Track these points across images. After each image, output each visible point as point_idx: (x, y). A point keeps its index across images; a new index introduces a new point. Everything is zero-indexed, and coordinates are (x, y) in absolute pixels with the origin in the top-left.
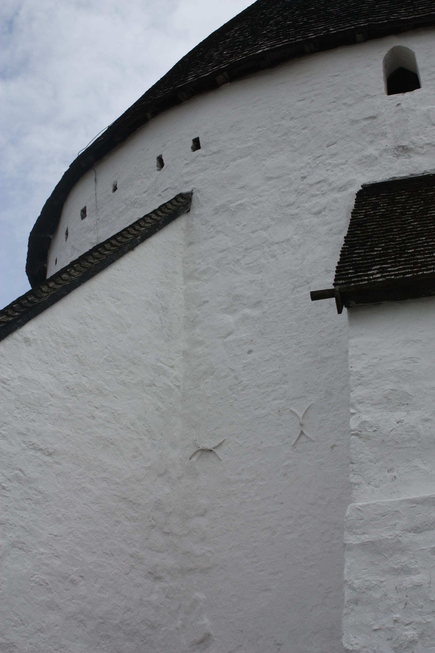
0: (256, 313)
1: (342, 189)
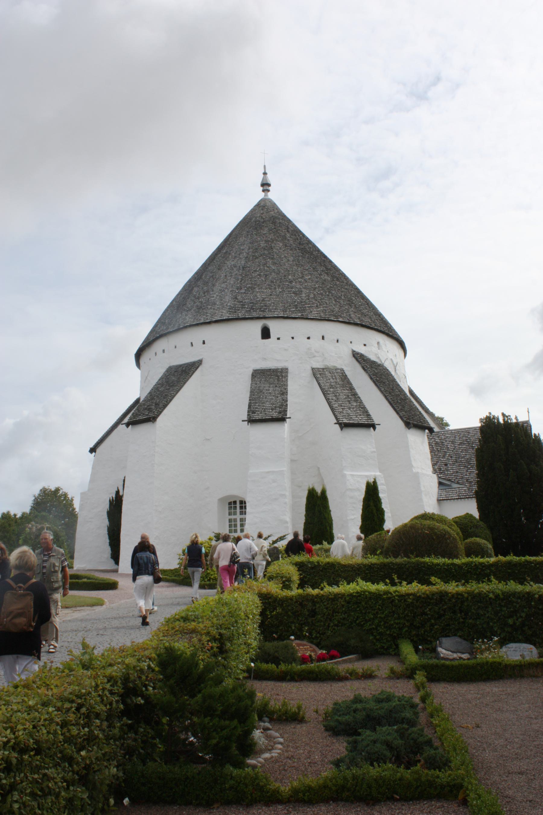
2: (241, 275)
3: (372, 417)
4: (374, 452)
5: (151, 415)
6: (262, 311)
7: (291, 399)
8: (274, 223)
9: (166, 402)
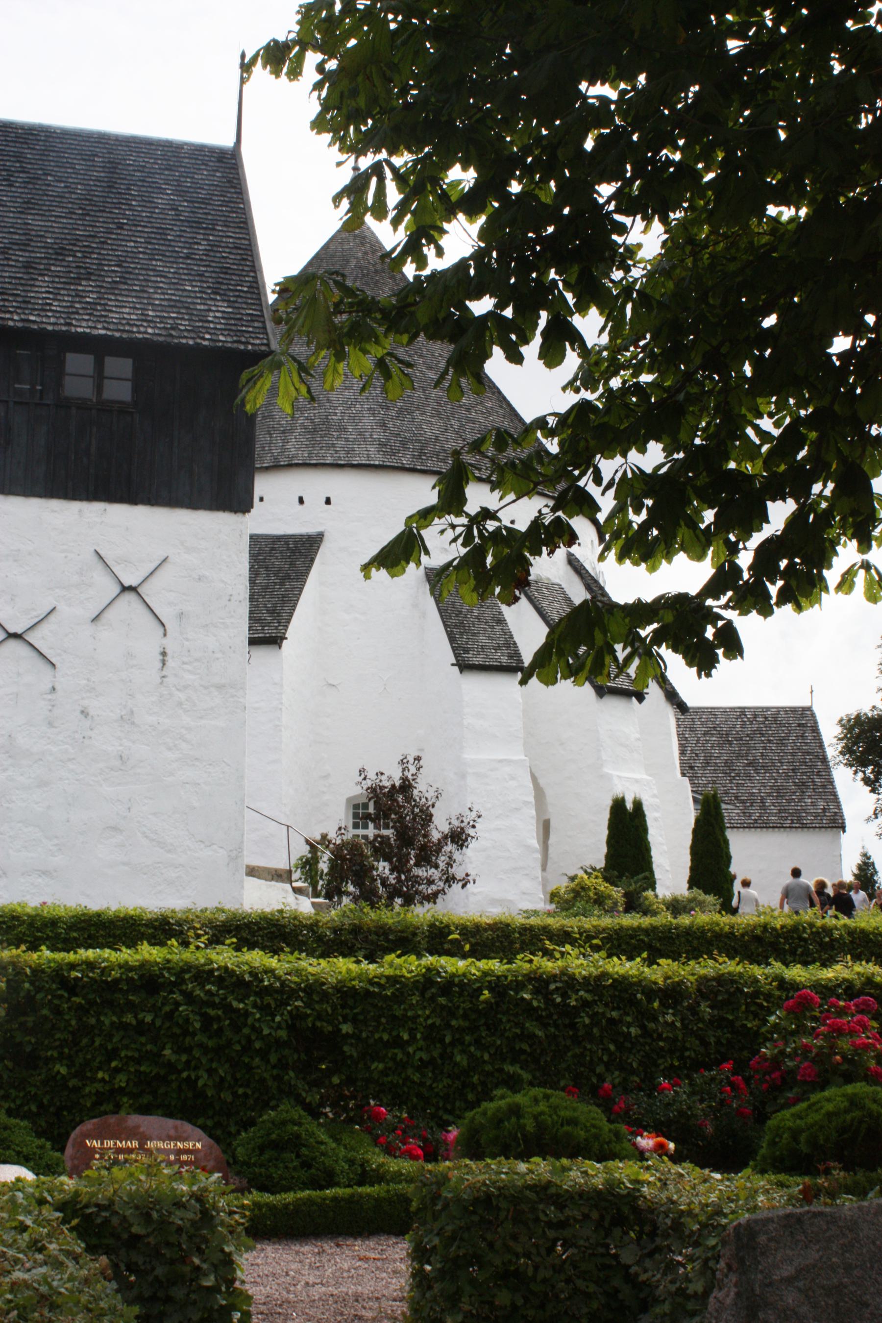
4: (638, 739)
5: (269, 632)
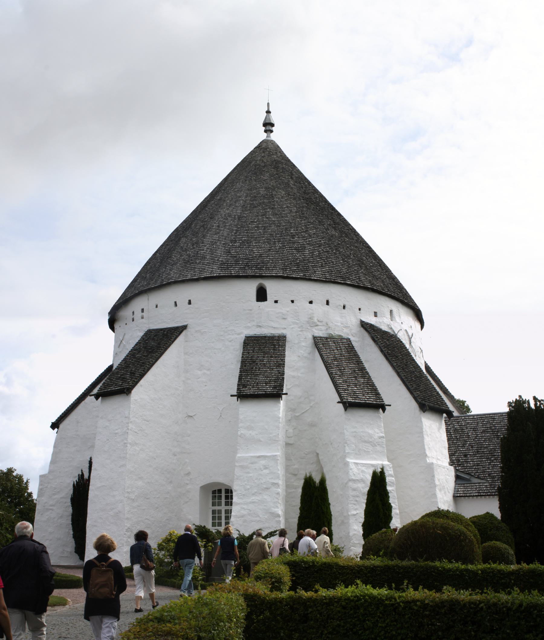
0: (208, 373)
1: (239, 334)
2: (236, 226)
3: (382, 396)
4: (383, 437)
5: (125, 385)
6: (258, 269)
7: (288, 372)
8: (276, 168)
9: (143, 371)
